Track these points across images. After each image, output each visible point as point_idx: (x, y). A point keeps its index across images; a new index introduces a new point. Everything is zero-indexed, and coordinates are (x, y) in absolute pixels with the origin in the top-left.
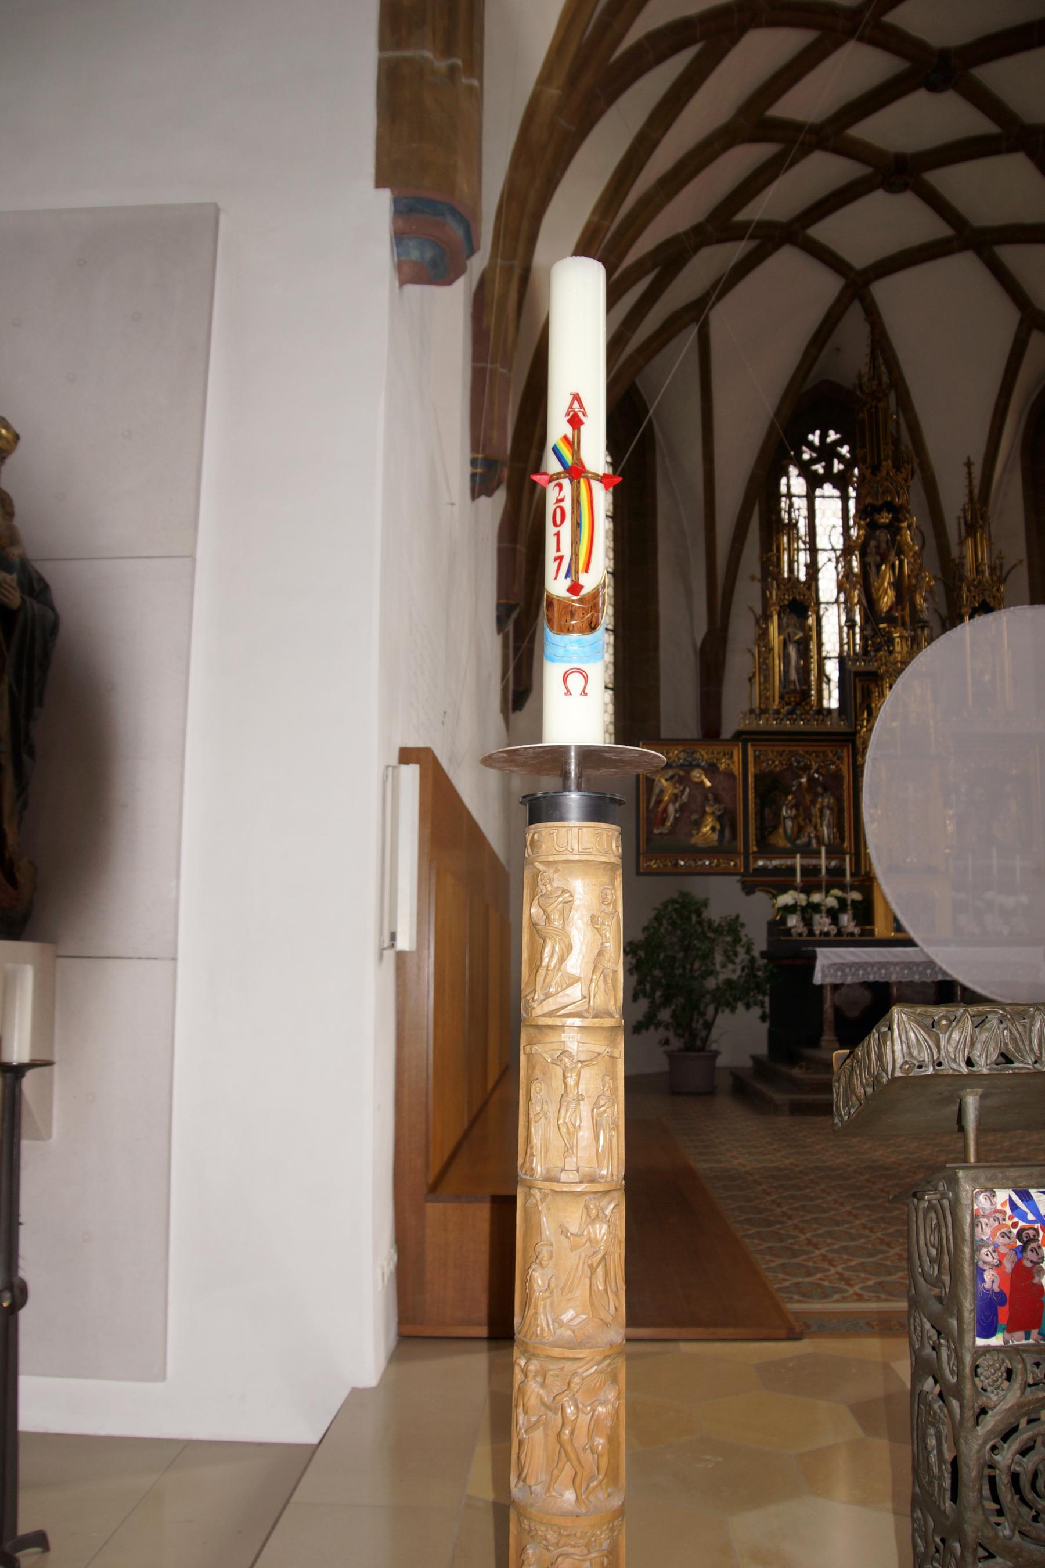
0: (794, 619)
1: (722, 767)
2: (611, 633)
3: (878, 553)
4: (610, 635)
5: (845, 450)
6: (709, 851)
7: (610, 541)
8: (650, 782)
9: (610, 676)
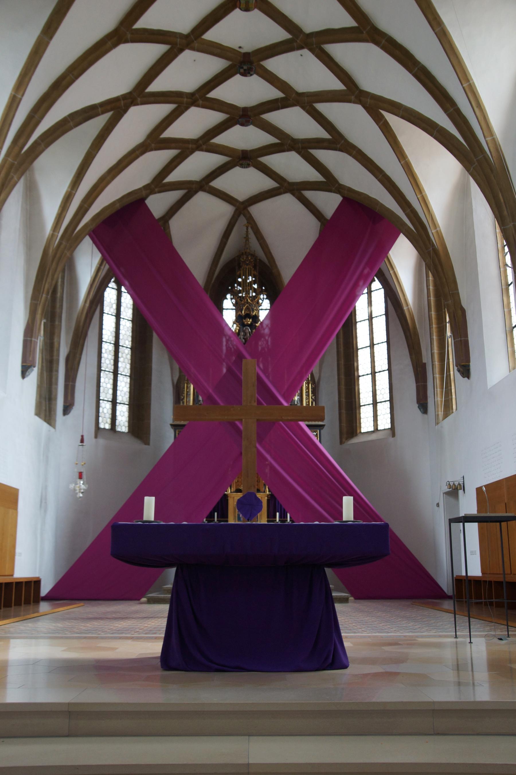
2: (128, 377)
3: (243, 338)
4: (127, 378)
5: (255, 286)
7: (130, 333)
9: (127, 398)
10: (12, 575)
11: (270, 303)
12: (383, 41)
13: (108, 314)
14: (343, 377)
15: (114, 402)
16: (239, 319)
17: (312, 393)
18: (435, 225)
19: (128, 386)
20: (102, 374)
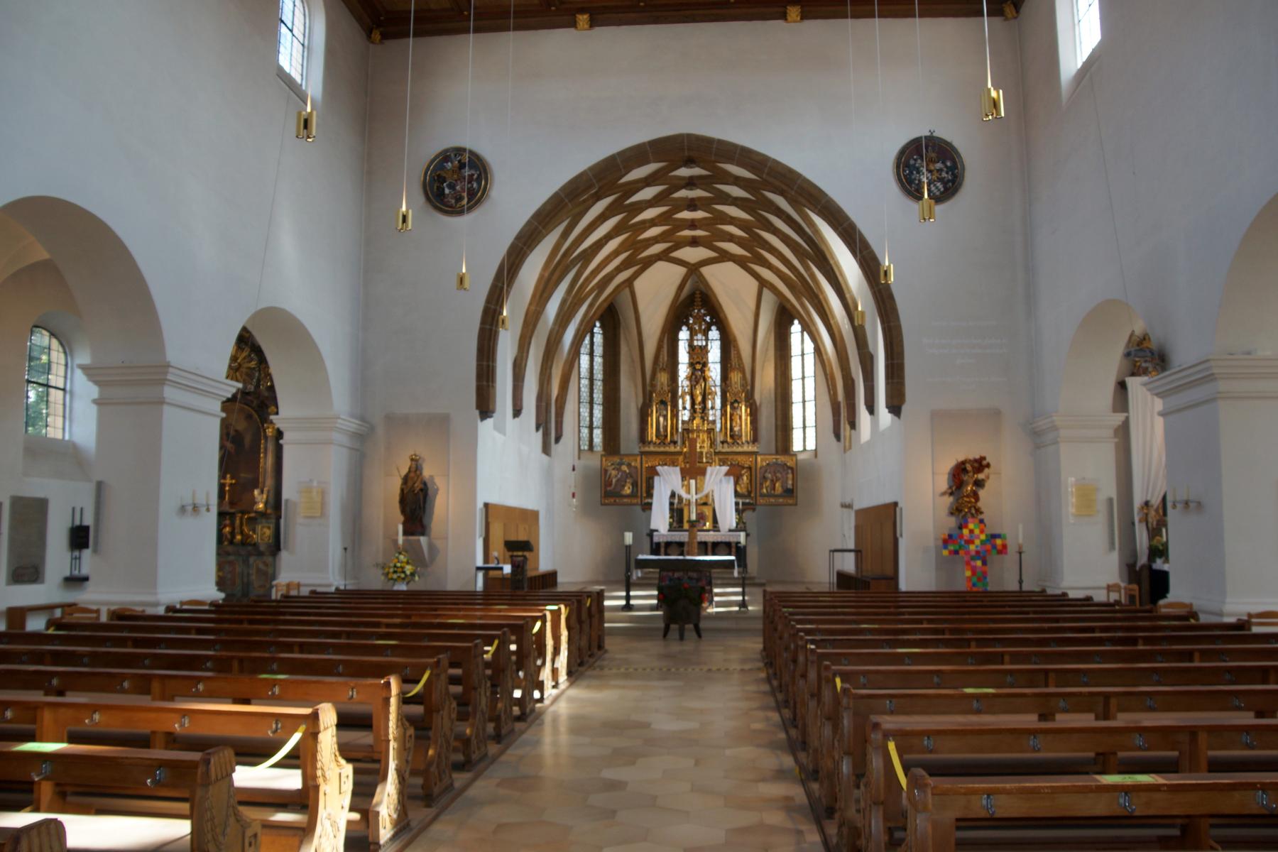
0: (662, 407)
1: (633, 464)
5: (708, 319)
6: (628, 496)
8: (606, 471)
10: (537, 568)
11: (720, 334)
12: (784, 217)
13: (584, 354)
14: (779, 404)
15: (591, 428)
16: (692, 365)
17: (751, 423)
18: (834, 317)
19: (601, 412)
20: (581, 405)
